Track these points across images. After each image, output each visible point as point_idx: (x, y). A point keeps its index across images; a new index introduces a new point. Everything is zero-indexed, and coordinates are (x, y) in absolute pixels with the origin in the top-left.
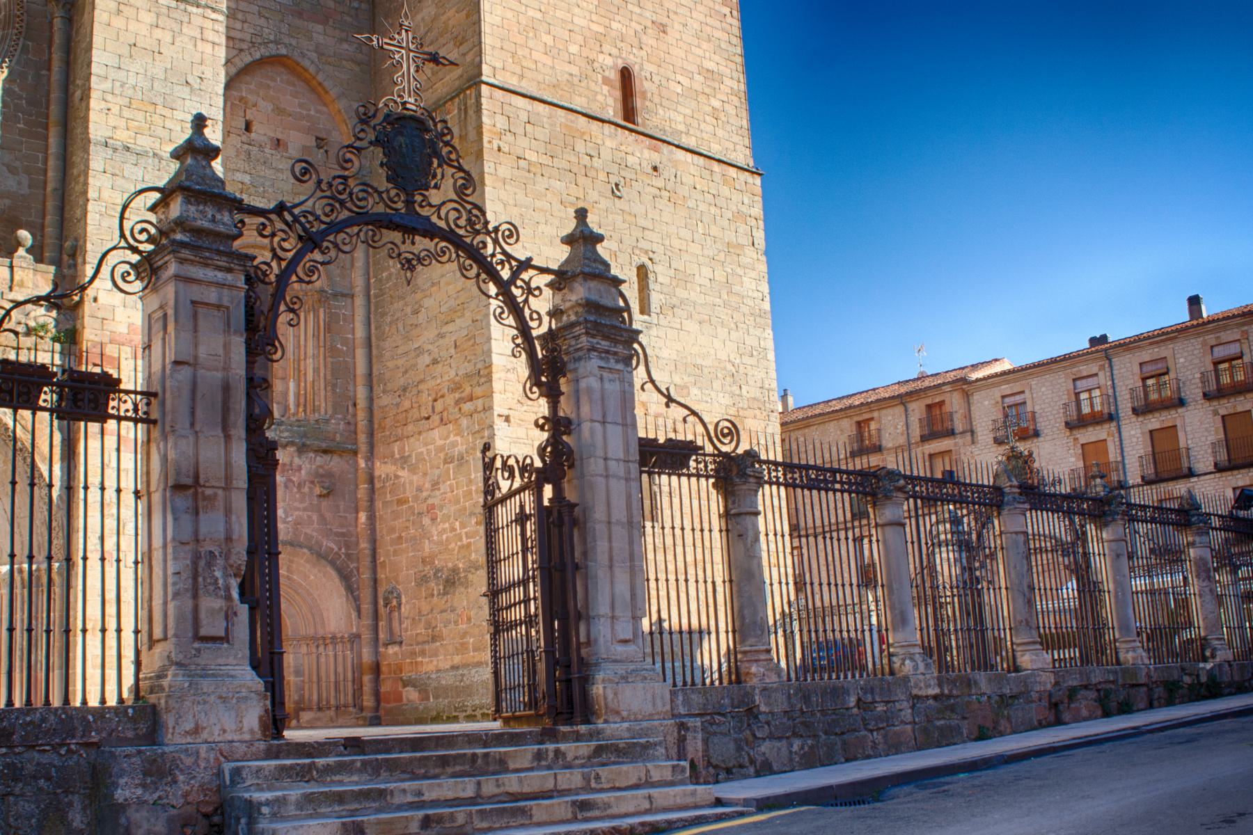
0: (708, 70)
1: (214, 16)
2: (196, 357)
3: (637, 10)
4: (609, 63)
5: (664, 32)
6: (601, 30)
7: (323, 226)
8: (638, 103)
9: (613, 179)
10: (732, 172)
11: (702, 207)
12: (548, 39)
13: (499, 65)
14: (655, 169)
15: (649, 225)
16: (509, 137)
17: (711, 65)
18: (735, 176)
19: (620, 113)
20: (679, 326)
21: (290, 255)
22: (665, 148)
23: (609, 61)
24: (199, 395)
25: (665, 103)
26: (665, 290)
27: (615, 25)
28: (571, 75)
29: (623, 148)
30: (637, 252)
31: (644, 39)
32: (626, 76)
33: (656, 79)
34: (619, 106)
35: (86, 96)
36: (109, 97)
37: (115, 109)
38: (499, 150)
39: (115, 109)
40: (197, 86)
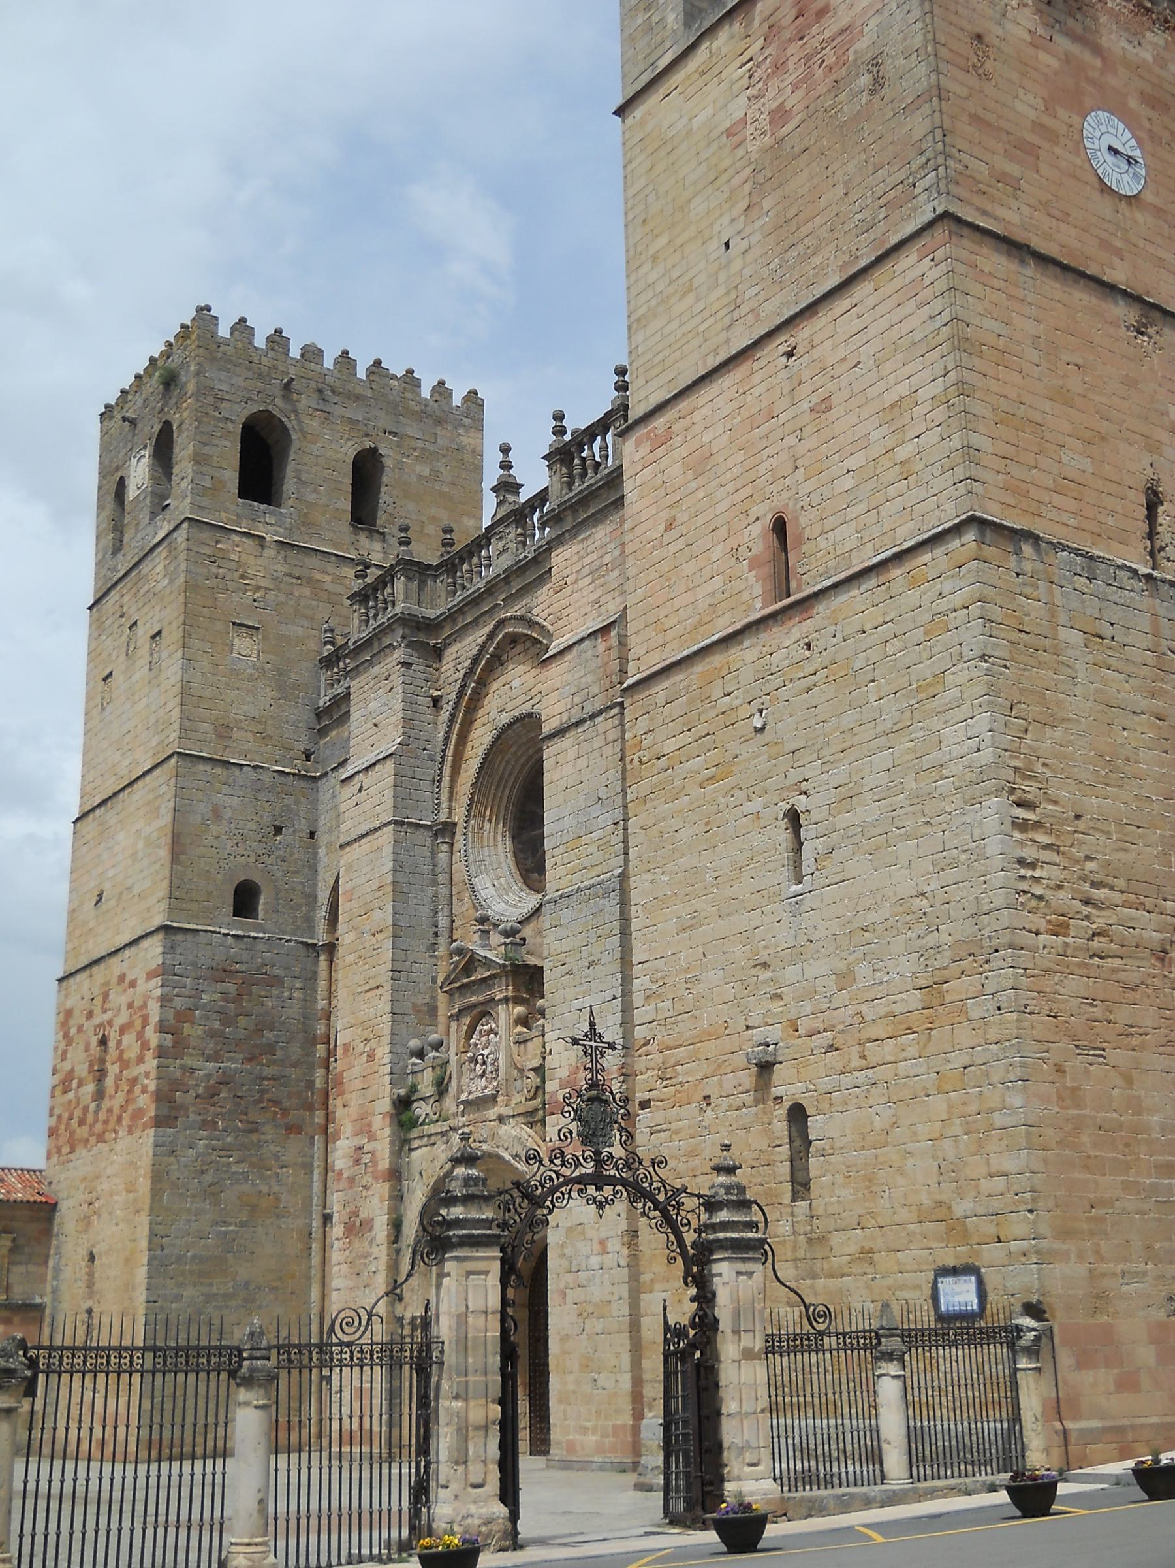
0: (892, 406)
4: (757, 536)
11: (874, 655)
14: (808, 646)
23: (757, 529)
28: (714, 593)
34: (770, 586)
38: (640, 762)
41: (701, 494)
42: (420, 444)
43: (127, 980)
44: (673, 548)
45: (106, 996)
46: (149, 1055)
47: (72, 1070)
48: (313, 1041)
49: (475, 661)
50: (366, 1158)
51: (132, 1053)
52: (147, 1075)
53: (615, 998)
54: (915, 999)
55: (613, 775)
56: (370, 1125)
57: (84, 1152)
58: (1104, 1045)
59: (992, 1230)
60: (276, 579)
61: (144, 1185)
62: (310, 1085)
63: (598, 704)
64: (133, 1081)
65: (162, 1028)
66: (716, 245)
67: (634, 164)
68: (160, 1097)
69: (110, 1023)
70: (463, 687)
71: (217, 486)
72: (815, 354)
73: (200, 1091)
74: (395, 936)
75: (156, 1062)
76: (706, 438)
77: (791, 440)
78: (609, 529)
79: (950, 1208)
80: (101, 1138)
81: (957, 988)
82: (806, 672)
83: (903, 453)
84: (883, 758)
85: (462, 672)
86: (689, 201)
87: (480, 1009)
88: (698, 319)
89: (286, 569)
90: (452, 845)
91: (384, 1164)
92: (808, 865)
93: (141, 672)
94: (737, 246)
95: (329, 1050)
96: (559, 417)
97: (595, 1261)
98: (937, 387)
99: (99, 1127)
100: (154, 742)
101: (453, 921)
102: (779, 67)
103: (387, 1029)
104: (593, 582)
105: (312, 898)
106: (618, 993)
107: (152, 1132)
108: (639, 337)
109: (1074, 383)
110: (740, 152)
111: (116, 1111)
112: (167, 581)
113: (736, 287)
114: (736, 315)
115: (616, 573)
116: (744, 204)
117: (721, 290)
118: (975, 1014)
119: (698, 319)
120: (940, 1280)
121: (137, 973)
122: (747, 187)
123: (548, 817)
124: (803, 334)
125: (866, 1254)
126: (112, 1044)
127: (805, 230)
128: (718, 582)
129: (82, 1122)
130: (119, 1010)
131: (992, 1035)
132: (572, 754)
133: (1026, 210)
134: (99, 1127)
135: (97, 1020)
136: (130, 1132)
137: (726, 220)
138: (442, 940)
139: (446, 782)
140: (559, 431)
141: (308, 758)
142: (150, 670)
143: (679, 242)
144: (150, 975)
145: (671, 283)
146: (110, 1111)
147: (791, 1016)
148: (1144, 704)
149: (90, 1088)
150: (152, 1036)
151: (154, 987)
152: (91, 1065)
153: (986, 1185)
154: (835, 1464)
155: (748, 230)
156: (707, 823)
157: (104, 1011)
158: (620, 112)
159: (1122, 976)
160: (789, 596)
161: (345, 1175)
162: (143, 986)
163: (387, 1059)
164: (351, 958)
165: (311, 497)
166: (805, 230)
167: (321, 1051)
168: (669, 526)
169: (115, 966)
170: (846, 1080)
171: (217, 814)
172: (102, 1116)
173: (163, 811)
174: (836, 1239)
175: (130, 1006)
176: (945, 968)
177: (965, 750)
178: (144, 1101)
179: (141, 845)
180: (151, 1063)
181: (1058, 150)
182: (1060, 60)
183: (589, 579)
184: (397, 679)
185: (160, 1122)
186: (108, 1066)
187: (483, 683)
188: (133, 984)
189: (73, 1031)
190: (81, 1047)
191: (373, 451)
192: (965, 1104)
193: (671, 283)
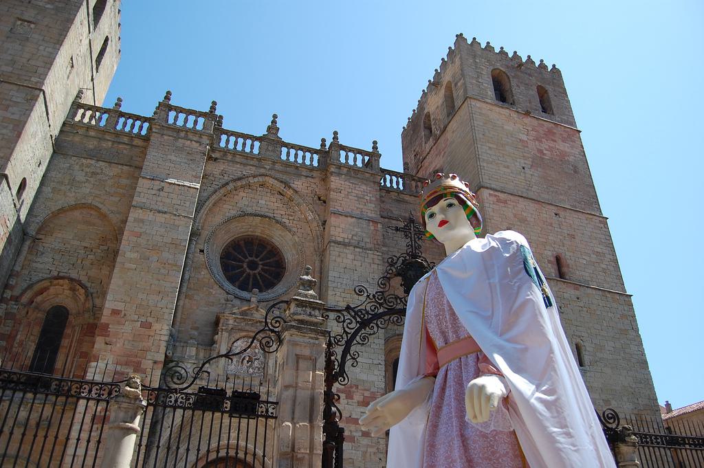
0: (597, 252)
1: (378, 254)
2: (297, 383)
3: (559, 230)
5: (574, 238)
7: (370, 316)
8: (565, 269)
14: (578, 299)
15: (578, 324)
17: (599, 250)
19: (558, 275)
20: (600, 371)
21: (353, 331)
22: (582, 288)
23: (550, 253)
24: (297, 403)
25: (579, 268)
26: (592, 354)
27: (550, 238)
29: (561, 290)
30: (575, 337)
31: (565, 242)
33: (573, 259)
34: (557, 272)
35: (327, 291)
37: (338, 294)
39: (338, 294)
40: (371, 282)
48: (7, 286)
49: (240, 179)
53: (380, 364)
56: (139, 363)
63: (368, 246)
70: (227, 184)
83: (604, 266)
100: (10, 69)
110: (526, 149)
124: (562, 213)
137: (522, 161)
138: (185, 285)
145: (499, 160)
183: (356, 198)
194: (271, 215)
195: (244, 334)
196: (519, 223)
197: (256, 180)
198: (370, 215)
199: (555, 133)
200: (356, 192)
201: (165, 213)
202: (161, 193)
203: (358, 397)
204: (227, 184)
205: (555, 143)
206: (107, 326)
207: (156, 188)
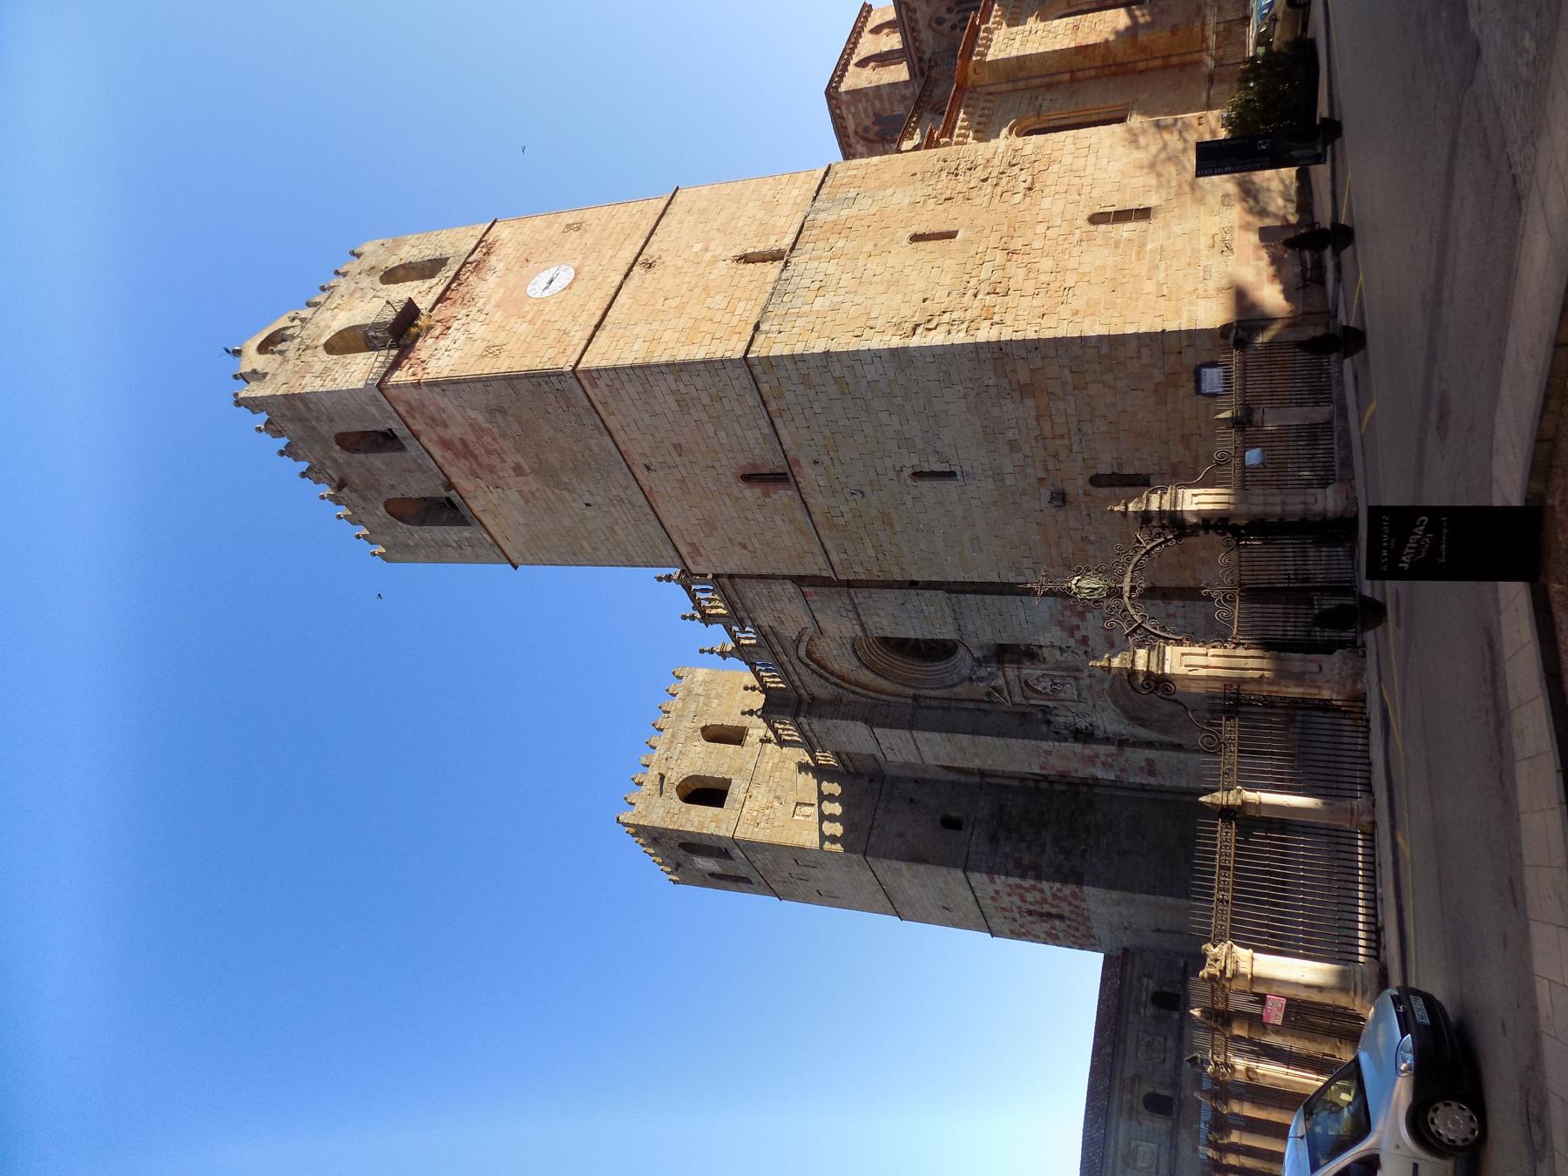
0: (679, 405)
1: (853, 593)
4: (751, 494)
5: (680, 446)
6: (726, 498)
8: (764, 471)
9: (849, 497)
10: (765, 388)
12: (769, 536)
13: (815, 567)
16: (866, 564)
18: (767, 386)
22: (791, 454)
23: (748, 493)
30: (903, 481)
32: (748, 478)
36: (933, 632)
39: (938, 631)
41: (726, 526)
42: (701, 705)
43: (994, 895)
44: (757, 546)
45: (1003, 909)
46: (1039, 886)
47: (1046, 932)
49: (821, 676)
50: (1109, 760)
51: (1038, 896)
52: (1051, 888)
54: (1030, 403)
55: (890, 594)
56: (1089, 757)
57: (1094, 930)
58: (1062, 288)
59: (1173, 357)
60: (769, 791)
61: (1116, 895)
62: (1063, 793)
64: (1055, 896)
65: (1023, 876)
66: (589, 512)
67: (544, 559)
68: (1064, 881)
69: (1019, 908)
70: (835, 684)
71: (715, 819)
72: (648, 451)
73: (1062, 857)
74: (979, 734)
75: (1044, 882)
76: (694, 522)
77: (697, 470)
78: (748, 590)
79: (1157, 384)
80: (1087, 919)
81: (1023, 376)
82: (830, 463)
83: (706, 400)
84: (884, 416)
85: (828, 684)
86: (564, 527)
87: (1023, 685)
88: (628, 524)
89: (764, 785)
90: (926, 697)
91: (1113, 749)
92: (945, 468)
93: (818, 873)
94: (588, 498)
95: (1044, 781)
96: (684, 618)
97: (1180, 622)
98: (670, 378)
99: (1080, 919)
100: (857, 868)
101: (972, 700)
102: (492, 470)
103: (1034, 742)
104: (778, 600)
105: (953, 784)
106: (1018, 598)
107: (1085, 888)
108: (637, 560)
109: (674, 303)
110: (537, 494)
111: (1071, 908)
112: (767, 854)
113: (611, 500)
114: (626, 501)
115: (773, 586)
116: (566, 494)
117: (612, 509)
118: (1039, 363)
119: (628, 524)
120: (1203, 392)
121: (990, 889)
122: (556, 491)
123: (912, 635)
125: (1185, 439)
126: (1032, 908)
127: (580, 458)
128: (778, 518)
129: (1077, 929)
130: (1012, 902)
131: (1052, 353)
132: (876, 619)
133: (576, 328)
134: (1080, 919)
135: (1017, 916)
136: (1085, 901)
137: (574, 505)
138: (983, 706)
139: (890, 698)
140: (693, 618)
141: (871, 781)
142: (816, 867)
143: (585, 534)
144: (992, 881)
145: (607, 539)
146: (1071, 912)
147: (1036, 481)
148: (861, 262)
149: (1057, 923)
150: (1028, 883)
151: (1000, 880)
152: (1043, 921)
153: (1145, 360)
154: (1317, 464)
155: (578, 491)
156: (917, 530)
157: (1012, 911)
158: (516, 568)
159: (1021, 277)
160: (786, 474)
161: (1119, 773)
162: (999, 888)
163: (1051, 744)
164: (989, 762)
165: (726, 766)
166: (580, 458)
167: (1043, 785)
168: (744, 547)
169: (984, 902)
170: (1075, 448)
171: (900, 835)
172: (1074, 917)
173: (897, 867)
174: (1175, 459)
175: (1009, 895)
176: (1010, 381)
177: (879, 365)
178: (1067, 890)
179: (916, 881)
180: (1045, 885)
181: (546, 311)
182: (497, 311)
184: (829, 722)
185: (1079, 883)
186: (1044, 911)
187: (832, 673)
188: (997, 892)
189: (1023, 930)
190: (1033, 926)
191: (704, 729)
192: (1094, 373)
193: (607, 539)
194: (848, 646)
195: (1025, 688)
196: (720, 530)
197: (810, 663)
198: (792, 590)
199: (439, 437)
200: (764, 602)
201: (917, 747)
202: (894, 747)
203: (1075, 621)
204: (835, 684)
205: (471, 444)
206: (1057, 772)
207: (892, 752)
